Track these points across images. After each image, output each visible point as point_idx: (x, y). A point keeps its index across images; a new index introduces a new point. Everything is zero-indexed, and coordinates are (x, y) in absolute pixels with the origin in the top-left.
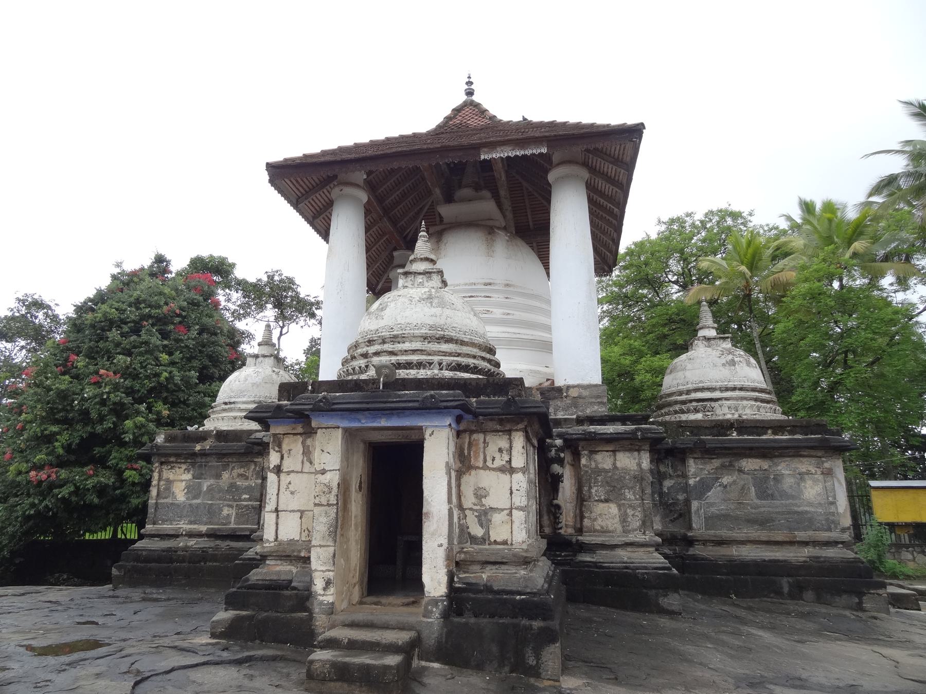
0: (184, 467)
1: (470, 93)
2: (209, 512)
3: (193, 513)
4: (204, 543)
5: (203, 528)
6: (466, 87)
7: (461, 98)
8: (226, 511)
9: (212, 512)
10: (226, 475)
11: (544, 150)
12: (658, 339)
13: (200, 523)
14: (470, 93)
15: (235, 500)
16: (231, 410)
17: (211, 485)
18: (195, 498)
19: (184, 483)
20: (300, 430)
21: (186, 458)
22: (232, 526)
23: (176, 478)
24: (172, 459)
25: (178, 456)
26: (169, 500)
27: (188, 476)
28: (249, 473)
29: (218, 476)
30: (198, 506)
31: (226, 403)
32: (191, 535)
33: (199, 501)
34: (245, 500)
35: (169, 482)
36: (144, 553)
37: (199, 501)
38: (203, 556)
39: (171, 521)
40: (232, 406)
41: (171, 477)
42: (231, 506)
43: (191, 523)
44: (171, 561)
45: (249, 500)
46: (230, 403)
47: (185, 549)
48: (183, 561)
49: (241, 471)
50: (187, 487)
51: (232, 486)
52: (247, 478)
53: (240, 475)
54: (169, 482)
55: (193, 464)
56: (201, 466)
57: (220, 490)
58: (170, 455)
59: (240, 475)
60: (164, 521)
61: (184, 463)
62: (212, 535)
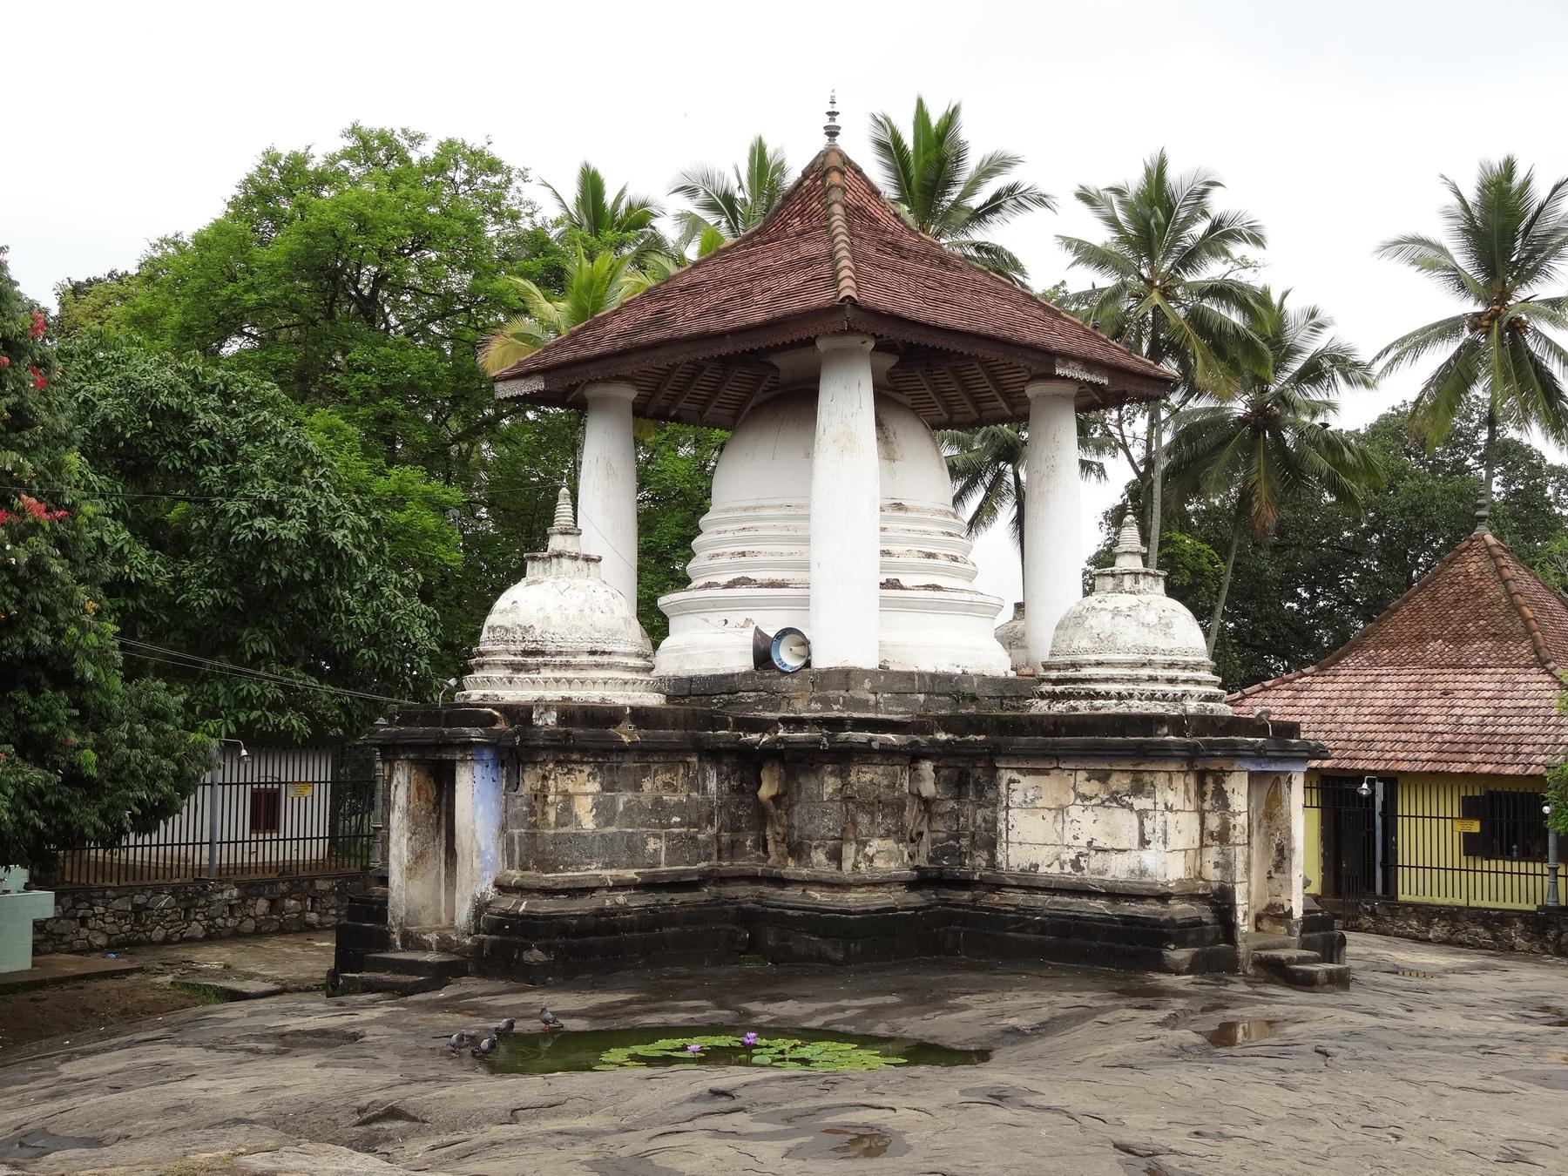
0: (587, 769)
1: (832, 133)
2: (629, 847)
3: (609, 849)
4: (639, 901)
5: (631, 874)
6: (826, 121)
7: (822, 142)
8: (652, 845)
9: (633, 849)
10: (647, 785)
11: (1106, 382)
12: (377, 419)
13: (620, 867)
14: (832, 133)
15: (663, 826)
16: (610, 666)
17: (629, 801)
18: (608, 823)
19: (590, 799)
20: (1185, 768)
21: (596, 756)
22: (663, 868)
23: (577, 789)
24: (575, 757)
25: (584, 751)
26: (570, 829)
27: (594, 787)
28: (678, 782)
29: (637, 787)
30: (612, 838)
31: (593, 653)
32: (621, 886)
33: (613, 829)
34: (676, 825)
35: (568, 797)
36: (575, 922)
37: (613, 829)
38: (652, 920)
39: (577, 865)
40: (605, 659)
41: (571, 788)
42: (657, 836)
43: (607, 866)
44: (613, 929)
45: (681, 825)
46: (604, 653)
47: (625, 909)
48: (631, 930)
49: (667, 777)
50: (596, 805)
51: (658, 801)
52: (675, 791)
53: (666, 785)
54: (568, 797)
55: (600, 766)
56: (610, 769)
57: (642, 810)
58: (572, 750)
59: (666, 785)
60: (567, 866)
61: (588, 763)
62: (649, 885)
